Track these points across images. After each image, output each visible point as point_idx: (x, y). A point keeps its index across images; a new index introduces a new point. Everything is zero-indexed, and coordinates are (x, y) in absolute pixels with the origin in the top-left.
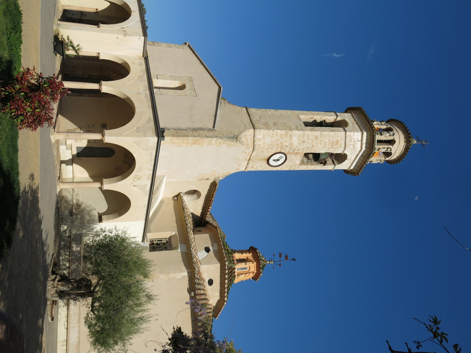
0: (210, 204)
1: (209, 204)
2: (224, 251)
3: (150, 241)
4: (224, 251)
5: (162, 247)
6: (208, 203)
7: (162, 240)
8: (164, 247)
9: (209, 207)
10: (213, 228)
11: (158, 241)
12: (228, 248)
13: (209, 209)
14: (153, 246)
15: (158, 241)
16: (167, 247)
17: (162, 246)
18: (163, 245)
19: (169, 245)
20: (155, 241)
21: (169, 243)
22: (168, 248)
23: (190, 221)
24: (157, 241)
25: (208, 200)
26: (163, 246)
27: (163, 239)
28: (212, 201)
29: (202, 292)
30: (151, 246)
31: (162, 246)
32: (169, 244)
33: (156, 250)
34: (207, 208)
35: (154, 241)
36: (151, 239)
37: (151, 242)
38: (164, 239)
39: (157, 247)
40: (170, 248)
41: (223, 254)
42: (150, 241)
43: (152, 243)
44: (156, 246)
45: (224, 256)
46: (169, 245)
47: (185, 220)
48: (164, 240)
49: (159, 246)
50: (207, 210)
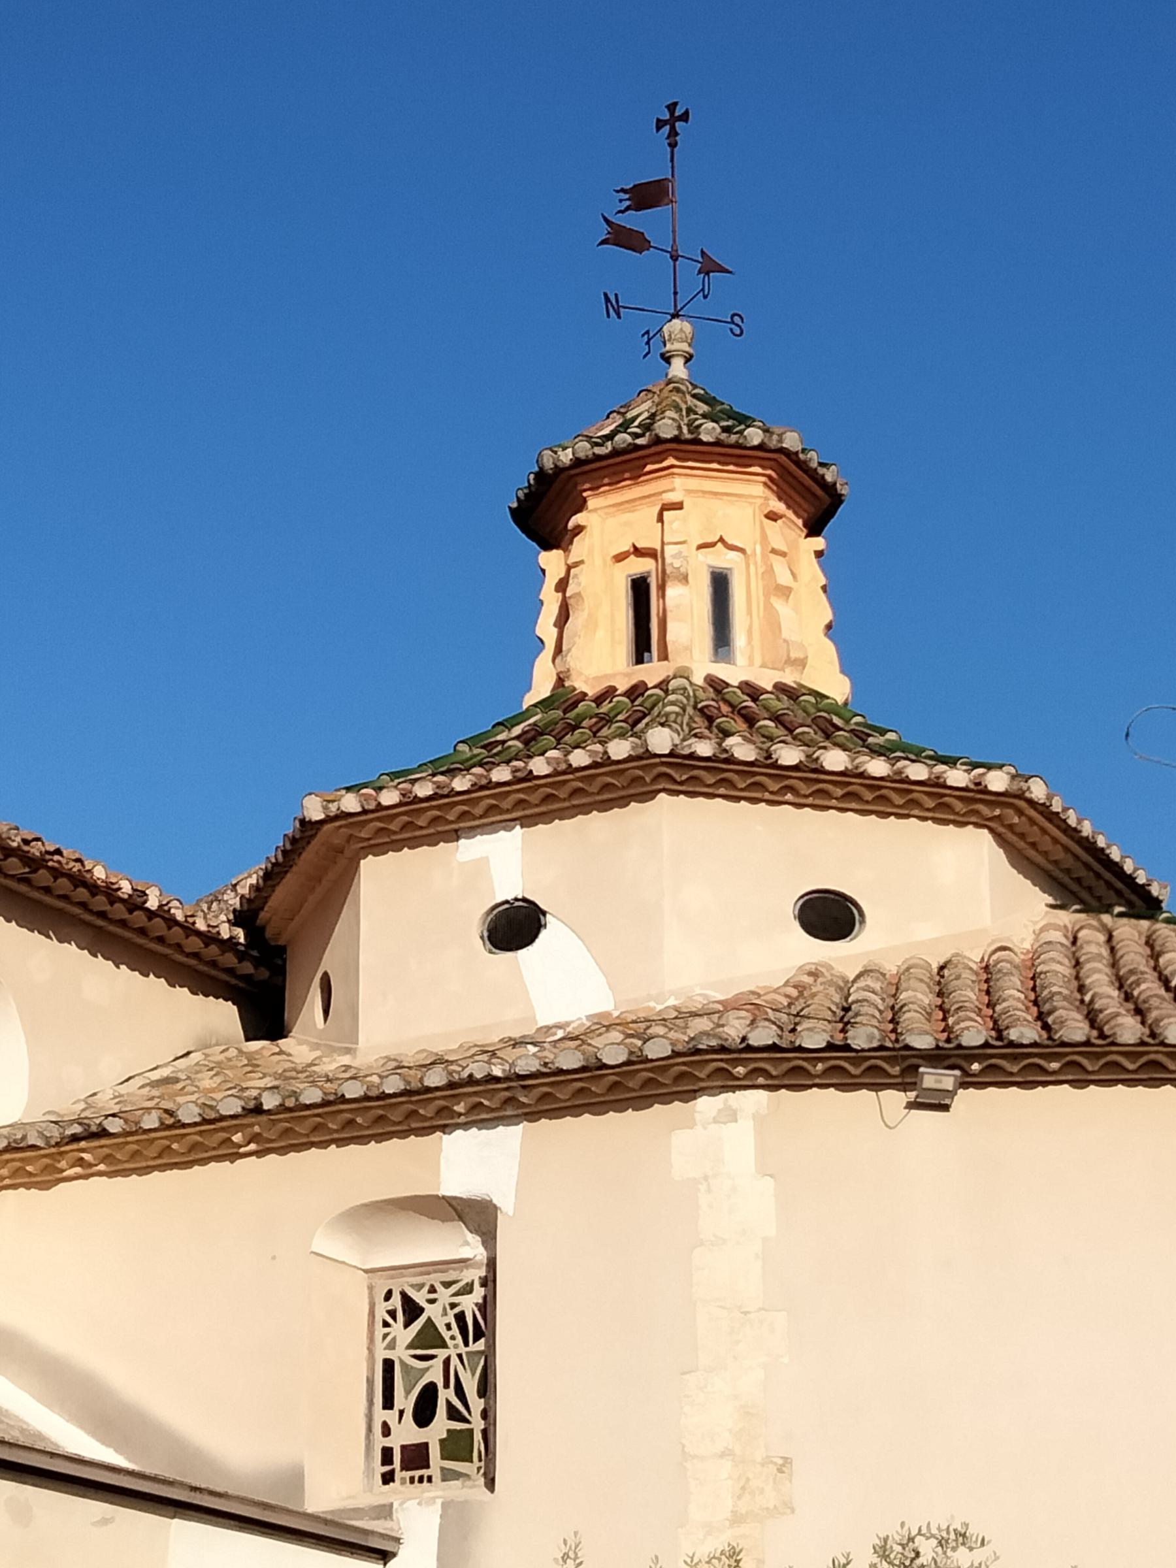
0: (70, 876)
1: (63, 881)
2: (539, 766)
3: (388, 1478)
4: (539, 766)
5: (455, 1361)
6: (47, 890)
7: (388, 1365)
8: (455, 1346)
9: (93, 888)
10: (309, 855)
11: (388, 1403)
12: (517, 730)
13: (110, 892)
14: (435, 1452)
15: (388, 1403)
16: (460, 1318)
17: (447, 1362)
18: (432, 1357)
19: (445, 1296)
20: (386, 1430)
21: (420, 1297)
22: (469, 1304)
23: (218, 1079)
24: (391, 1416)
25: (23, 888)
26: (442, 1354)
27: (381, 1354)
28: (35, 849)
29: (918, 996)
30: (434, 1470)
31: (447, 1362)
32: (432, 1290)
33: (478, 1424)
34: (100, 903)
35: (387, 1442)
36: (369, 1471)
37: (399, 1475)
38: (380, 1345)
39: (453, 1414)
40: (468, 1289)
41: (570, 769)
42: (388, 1478)
43: (405, 1467)
44: (441, 1424)
45: (595, 765)
46: (445, 1296)
47: (205, 1121)
48: (392, 1346)
49: (446, 1395)
50: (119, 911)
